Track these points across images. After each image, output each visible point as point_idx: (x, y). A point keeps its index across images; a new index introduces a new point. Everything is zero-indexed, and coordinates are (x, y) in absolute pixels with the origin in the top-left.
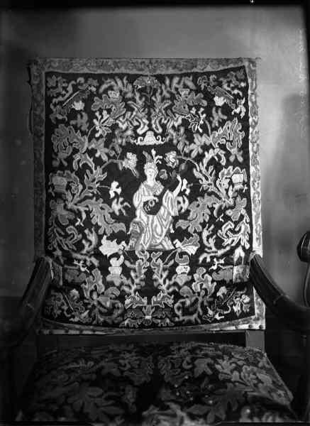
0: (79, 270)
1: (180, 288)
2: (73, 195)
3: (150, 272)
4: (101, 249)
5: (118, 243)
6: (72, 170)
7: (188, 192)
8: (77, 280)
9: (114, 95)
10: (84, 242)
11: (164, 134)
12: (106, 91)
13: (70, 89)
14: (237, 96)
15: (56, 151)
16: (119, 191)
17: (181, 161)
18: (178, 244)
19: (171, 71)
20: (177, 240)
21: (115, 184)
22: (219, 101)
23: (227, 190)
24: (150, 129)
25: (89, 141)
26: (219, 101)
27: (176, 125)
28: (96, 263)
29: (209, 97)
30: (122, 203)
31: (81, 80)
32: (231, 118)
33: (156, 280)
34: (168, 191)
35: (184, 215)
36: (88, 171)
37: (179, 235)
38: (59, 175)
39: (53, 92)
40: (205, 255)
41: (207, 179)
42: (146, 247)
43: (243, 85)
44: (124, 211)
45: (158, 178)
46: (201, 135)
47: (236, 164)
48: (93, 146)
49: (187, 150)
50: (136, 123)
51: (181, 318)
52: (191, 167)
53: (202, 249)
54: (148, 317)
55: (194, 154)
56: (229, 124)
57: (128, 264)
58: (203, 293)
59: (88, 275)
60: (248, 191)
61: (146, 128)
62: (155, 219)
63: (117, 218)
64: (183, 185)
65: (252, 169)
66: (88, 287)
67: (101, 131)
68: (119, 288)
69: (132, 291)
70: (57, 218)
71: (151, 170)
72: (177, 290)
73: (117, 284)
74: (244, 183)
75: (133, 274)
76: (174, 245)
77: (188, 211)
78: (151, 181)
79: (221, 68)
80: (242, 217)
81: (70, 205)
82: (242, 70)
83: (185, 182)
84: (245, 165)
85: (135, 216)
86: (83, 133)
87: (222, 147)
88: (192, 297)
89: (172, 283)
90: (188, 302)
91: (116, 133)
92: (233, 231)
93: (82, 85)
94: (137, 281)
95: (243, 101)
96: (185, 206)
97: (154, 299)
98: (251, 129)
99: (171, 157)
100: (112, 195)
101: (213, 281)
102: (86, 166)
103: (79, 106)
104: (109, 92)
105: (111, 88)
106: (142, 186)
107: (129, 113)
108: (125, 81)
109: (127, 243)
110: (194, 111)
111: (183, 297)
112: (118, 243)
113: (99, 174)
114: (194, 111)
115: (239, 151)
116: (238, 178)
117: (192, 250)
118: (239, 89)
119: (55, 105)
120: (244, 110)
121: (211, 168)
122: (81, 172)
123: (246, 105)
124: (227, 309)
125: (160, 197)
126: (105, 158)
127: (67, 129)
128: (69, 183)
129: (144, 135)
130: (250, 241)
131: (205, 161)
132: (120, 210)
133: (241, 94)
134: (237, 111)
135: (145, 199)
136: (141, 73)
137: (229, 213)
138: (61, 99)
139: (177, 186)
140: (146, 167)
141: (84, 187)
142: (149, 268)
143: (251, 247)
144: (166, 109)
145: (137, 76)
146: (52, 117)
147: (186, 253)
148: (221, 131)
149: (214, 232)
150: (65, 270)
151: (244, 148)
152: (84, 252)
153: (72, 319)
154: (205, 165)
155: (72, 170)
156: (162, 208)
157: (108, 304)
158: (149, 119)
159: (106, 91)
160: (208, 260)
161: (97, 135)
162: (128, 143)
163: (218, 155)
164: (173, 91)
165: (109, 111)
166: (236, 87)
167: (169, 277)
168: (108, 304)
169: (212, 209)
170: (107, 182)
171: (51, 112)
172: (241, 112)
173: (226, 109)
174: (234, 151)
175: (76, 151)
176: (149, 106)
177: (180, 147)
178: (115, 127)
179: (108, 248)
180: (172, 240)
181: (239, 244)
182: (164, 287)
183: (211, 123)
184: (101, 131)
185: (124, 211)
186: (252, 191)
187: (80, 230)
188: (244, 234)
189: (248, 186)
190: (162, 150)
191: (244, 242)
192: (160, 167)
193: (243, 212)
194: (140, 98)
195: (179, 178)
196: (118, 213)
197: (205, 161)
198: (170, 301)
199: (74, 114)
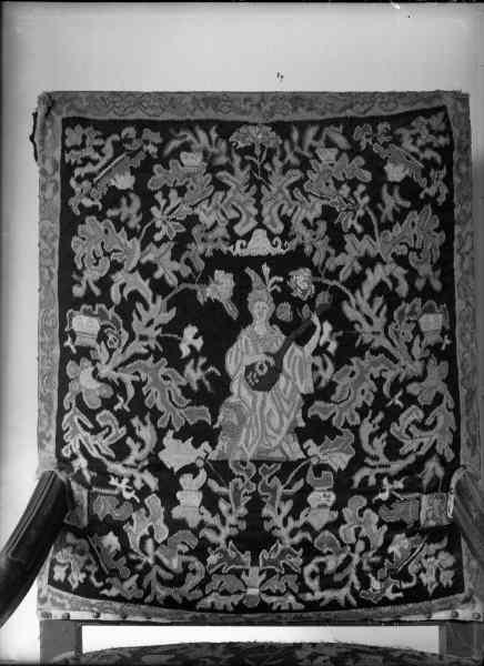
0: (120, 497)
1: (315, 534)
2: (111, 351)
3: (256, 504)
4: (163, 456)
5: (196, 445)
6: (109, 304)
7: (332, 347)
8: (117, 515)
9: (193, 161)
10: (129, 441)
11: (285, 236)
13: (109, 149)
14: (429, 165)
15: (79, 267)
16: (199, 344)
17: (320, 287)
18: (313, 449)
20: (310, 442)
21: (190, 331)
22: (395, 173)
23: (410, 345)
24: (261, 225)
25: (143, 248)
26: (395, 173)
27: (311, 218)
28: (153, 483)
29: (376, 164)
30: (204, 368)
31: (130, 131)
32: (418, 206)
33: (268, 519)
34: (293, 345)
35: (324, 392)
36: (139, 306)
37: (315, 430)
38: (86, 313)
39: (72, 157)
40: (365, 472)
41: (369, 321)
42: (250, 455)
43: (442, 141)
44: (207, 383)
45: (273, 320)
46: (360, 237)
47: (427, 293)
48: (150, 257)
49: (331, 266)
50: (233, 214)
51: (318, 595)
52: (339, 297)
53: (358, 460)
54: (251, 591)
55: (344, 275)
56: (413, 216)
57: (215, 486)
58: (360, 546)
59: (137, 506)
60: (452, 347)
61: (253, 223)
62: (267, 400)
63: (194, 396)
64: (324, 333)
65: (459, 305)
66: (135, 532)
67: (166, 228)
69: (221, 539)
70: (79, 398)
71: (260, 306)
72: (310, 539)
73: (193, 522)
74: (443, 332)
75: (223, 506)
76: (305, 452)
77: (332, 385)
78: (260, 326)
79: (401, 109)
80: (438, 399)
81: (105, 371)
82: (441, 115)
83: (327, 327)
84: (444, 297)
85: (230, 394)
86: (132, 234)
87: (401, 261)
88: (339, 553)
89: (300, 523)
90: (332, 564)
91: (195, 231)
92: (421, 426)
93: (129, 141)
94: (231, 520)
95: (444, 172)
96: (327, 374)
97: (264, 554)
98: (457, 229)
99: (301, 280)
100: (185, 351)
101: (380, 524)
102: (135, 296)
103: (124, 181)
104: (183, 155)
105: (186, 147)
106: (244, 335)
107: (220, 195)
108: (214, 135)
109: (213, 445)
110: (345, 190)
111: (320, 554)
112: (196, 445)
113: (158, 312)
114: (345, 190)
115: (434, 270)
116: (432, 322)
117: (340, 460)
118: (435, 149)
119: (79, 180)
120: (444, 190)
121: (379, 301)
122: (127, 308)
123: (448, 181)
124: (409, 579)
125: (278, 356)
126: (172, 281)
127: (102, 226)
128: (103, 327)
129: (248, 237)
130: (456, 446)
131: (368, 287)
132: (200, 382)
133: (439, 159)
134: (431, 191)
135: (248, 361)
136: (245, 118)
137: (413, 388)
138: (90, 168)
139: (313, 333)
140: (251, 297)
141: (132, 337)
142: (255, 495)
143: (457, 457)
144: (291, 187)
145: (237, 125)
146: (73, 202)
147: (326, 467)
148: (398, 230)
149: (384, 426)
150: (92, 497)
151: (444, 264)
152: (130, 461)
153: (105, 592)
154: (367, 296)
155: (109, 304)
156: (282, 379)
157: (175, 564)
158: (259, 206)
159: (176, 154)
160: (372, 481)
161: (158, 237)
162: (217, 252)
163: (391, 277)
164: (307, 154)
165: (182, 191)
166: (430, 145)
167: (295, 514)
168: (175, 564)
169: (380, 381)
170: (175, 327)
171: (72, 193)
172: (438, 194)
173: (408, 188)
174: (425, 269)
175: (116, 267)
176: (258, 180)
177: (317, 260)
178: (192, 221)
179: (177, 454)
180: (301, 442)
181: (432, 451)
182: (284, 532)
183: (378, 213)
184: (166, 228)
185: (207, 383)
186: (459, 346)
187: (123, 418)
188: (441, 432)
189: (452, 338)
190: (282, 265)
191: (444, 447)
192: (278, 298)
193: (443, 388)
194: (242, 167)
195: (315, 320)
196: (195, 387)
197: (368, 287)
198: (296, 561)
199: (113, 197)
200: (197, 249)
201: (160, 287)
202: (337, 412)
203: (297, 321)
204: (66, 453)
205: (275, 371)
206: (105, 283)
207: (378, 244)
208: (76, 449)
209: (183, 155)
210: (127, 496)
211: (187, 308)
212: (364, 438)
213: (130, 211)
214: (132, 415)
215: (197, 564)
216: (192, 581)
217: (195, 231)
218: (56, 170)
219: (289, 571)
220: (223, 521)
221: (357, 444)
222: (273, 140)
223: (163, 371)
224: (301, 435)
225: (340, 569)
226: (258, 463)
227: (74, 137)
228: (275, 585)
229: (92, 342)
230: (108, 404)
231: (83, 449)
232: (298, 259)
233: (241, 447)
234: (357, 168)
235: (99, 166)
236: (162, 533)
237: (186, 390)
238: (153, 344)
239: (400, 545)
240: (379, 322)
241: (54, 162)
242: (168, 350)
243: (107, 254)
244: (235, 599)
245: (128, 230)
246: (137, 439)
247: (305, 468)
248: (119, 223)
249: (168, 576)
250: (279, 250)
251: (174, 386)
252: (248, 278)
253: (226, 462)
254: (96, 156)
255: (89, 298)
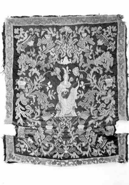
6: (28, 77)
12: (43, 36)
15: (20, 68)
16: (51, 86)
19: (78, 23)
20: (78, 112)
22: (100, 43)
28: (40, 123)
32: (106, 51)
33: (69, 133)
36: (36, 77)
47: (108, 73)
49: (83, 66)
52: (85, 75)
53: (90, 118)
54: (66, 152)
68: (51, 136)
71: (66, 77)
76: (77, 114)
77: (84, 98)
81: (27, 95)
88: (85, 142)
89: (76, 134)
90: (84, 145)
96: (82, 95)
99: (76, 71)
100: (48, 88)
102: (35, 74)
103: (31, 44)
111: (81, 142)
113: (42, 79)
116: (110, 81)
117: (85, 117)
122: (33, 77)
128: (27, 83)
137: (103, 99)
139: (77, 86)
145: (61, 27)
147: (83, 119)
148: (99, 58)
154: (92, 75)
155: (28, 77)
159: (43, 36)
161: (41, 59)
168: (47, 145)
175: (30, 68)
177: (80, 65)
178: (48, 54)
180: (76, 112)
183: (95, 53)
187: (33, 107)
190: (71, 66)
197: (92, 72)
199: (28, 49)
201: (42, 72)
206: (27, 72)
208: (20, 116)
211: (48, 78)
212: (91, 111)
215: (52, 145)
216: (51, 149)
218: (12, 40)
222: (70, 31)
225: (86, 146)
227: (16, 31)
230: (29, 103)
231: (22, 116)
232: (76, 65)
234: (91, 41)
237: (48, 99)
242: (43, 89)
246: (36, 112)
249: (45, 148)
250: (70, 62)
251: (46, 98)
252: (63, 70)
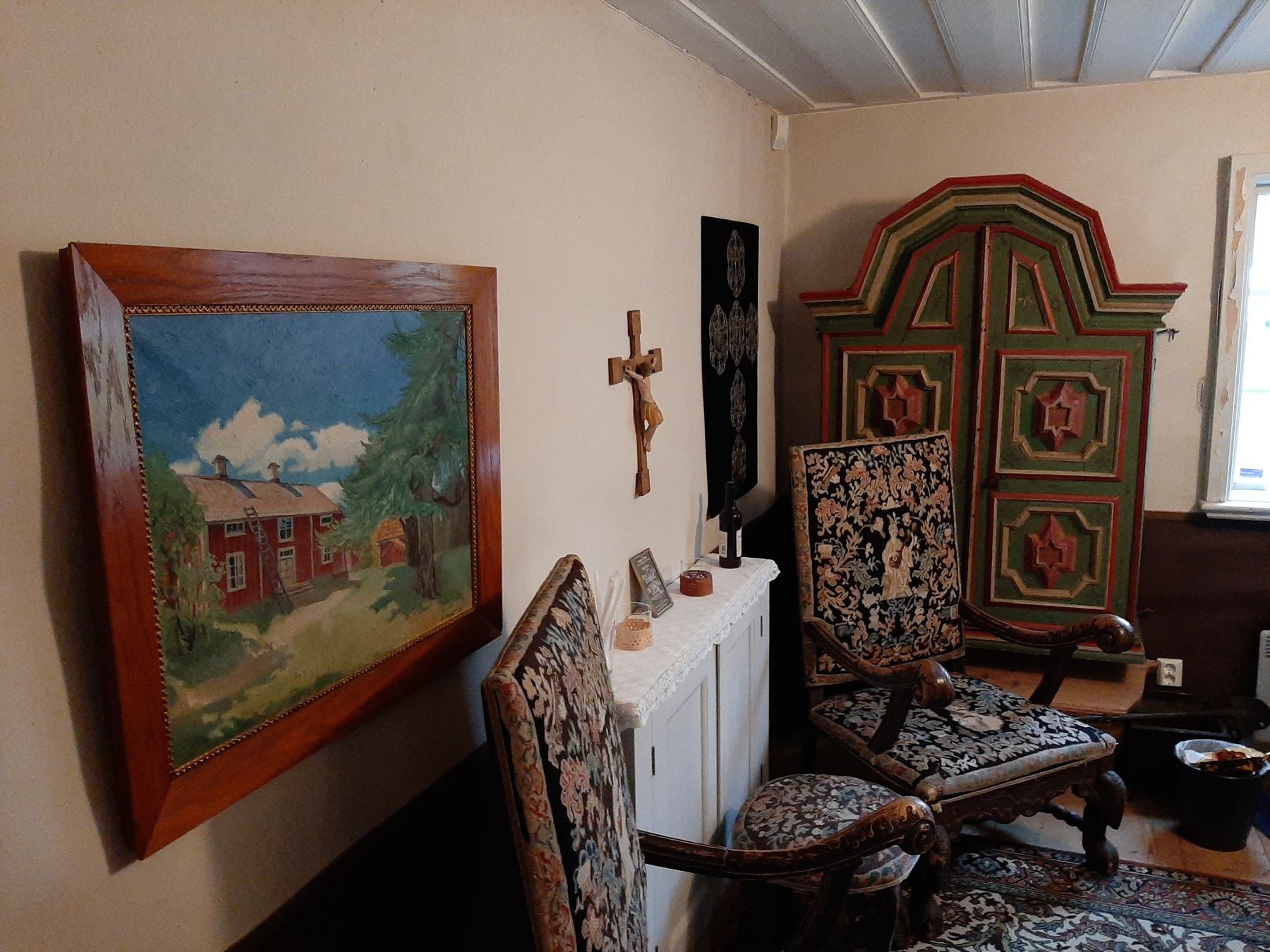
0: (848, 625)
1: (918, 626)
2: (838, 559)
5: (875, 595)
7: (918, 547)
10: (850, 597)
13: (826, 464)
15: (821, 522)
16: (872, 551)
17: (913, 521)
21: (869, 545)
24: (890, 495)
25: (848, 510)
28: (860, 615)
29: (926, 463)
30: (875, 561)
35: (917, 566)
36: (849, 537)
38: (826, 543)
42: (894, 596)
46: (924, 497)
48: (851, 514)
50: (880, 491)
52: (919, 524)
53: (930, 595)
55: (920, 515)
61: (888, 494)
67: (857, 501)
71: (893, 530)
75: (886, 620)
81: (836, 568)
86: (843, 504)
94: (890, 625)
96: (917, 558)
97: (902, 638)
99: (906, 518)
100: (867, 555)
101: (939, 619)
102: (847, 533)
103: (836, 479)
104: (856, 463)
105: (856, 459)
108: (865, 452)
110: (918, 475)
112: (875, 595)
113: (856, 539)
114: (918, 475)
119: (816, 481)
125: (900, 552)
126: (861, 524)
127: (829, 502)
128: (834, 548)
129: (886, 501)
131: (928, 520)
138: (820, 475)
144: (899, 475)
146: (814, 493)
148: (936, 493)
149: (937, 578)
150: (836, 628)
152: (851, 607)
155: (836, 537)
158: (889, 486)
161: (853, 505)
162: (876, 509)
163: (936, 514)
165: (859, 481)
167: (911, 619)
168: (869, 649)
169: (934, 559)
170: (863, 545)
174: (946, 509)
175: (838, 520)
177: (911, 509)
178: (865, 496)
179: (869, 600)
181: (952, 587)
182: (908, 627)
183: (930, 487)
184: (857, 501)
187: (847, 588)
197: (928, 520)
199: (833, 488)
200: (869, 508)
201: (856, 527)
202: (922, 574)
203: (906, 535)
204: (820, 609)
205: (900, 558)
206: (833, 528)
207: (930, 500)
208: (827, 606)
209: (856, 463)
210: (851, 623)
211: (868, 536)
212: (931, 583)
213: (840, 494)
214: (850, 586)
215: (878, 647)
217: (867, 500)
218: (804, 476)
219: (909, 644)
220: (887, 626)
221: (929, 587)
223: (860, 565)
224: (911, 585)
226: (897, 599)
228: (905, 649)
229: (830, 556)
230: (839, 583)
231: (830, 606)
233: (891, 594)
235: (824, 473)
236: (866, 637)
237: (869, 572)
238: (855, 553)
239: (945, 627)
240: (933, 533)
241: (802, 473)
242: (861, 555)
243: (833, 515)
244: (890, 659)
245: (841, 502)
246: (853, 596)
247: (913, 600)
248: (837, 500)
250: (898, 506)
253: (886, 601)
254: (822, 468)
255: (826, 535)
